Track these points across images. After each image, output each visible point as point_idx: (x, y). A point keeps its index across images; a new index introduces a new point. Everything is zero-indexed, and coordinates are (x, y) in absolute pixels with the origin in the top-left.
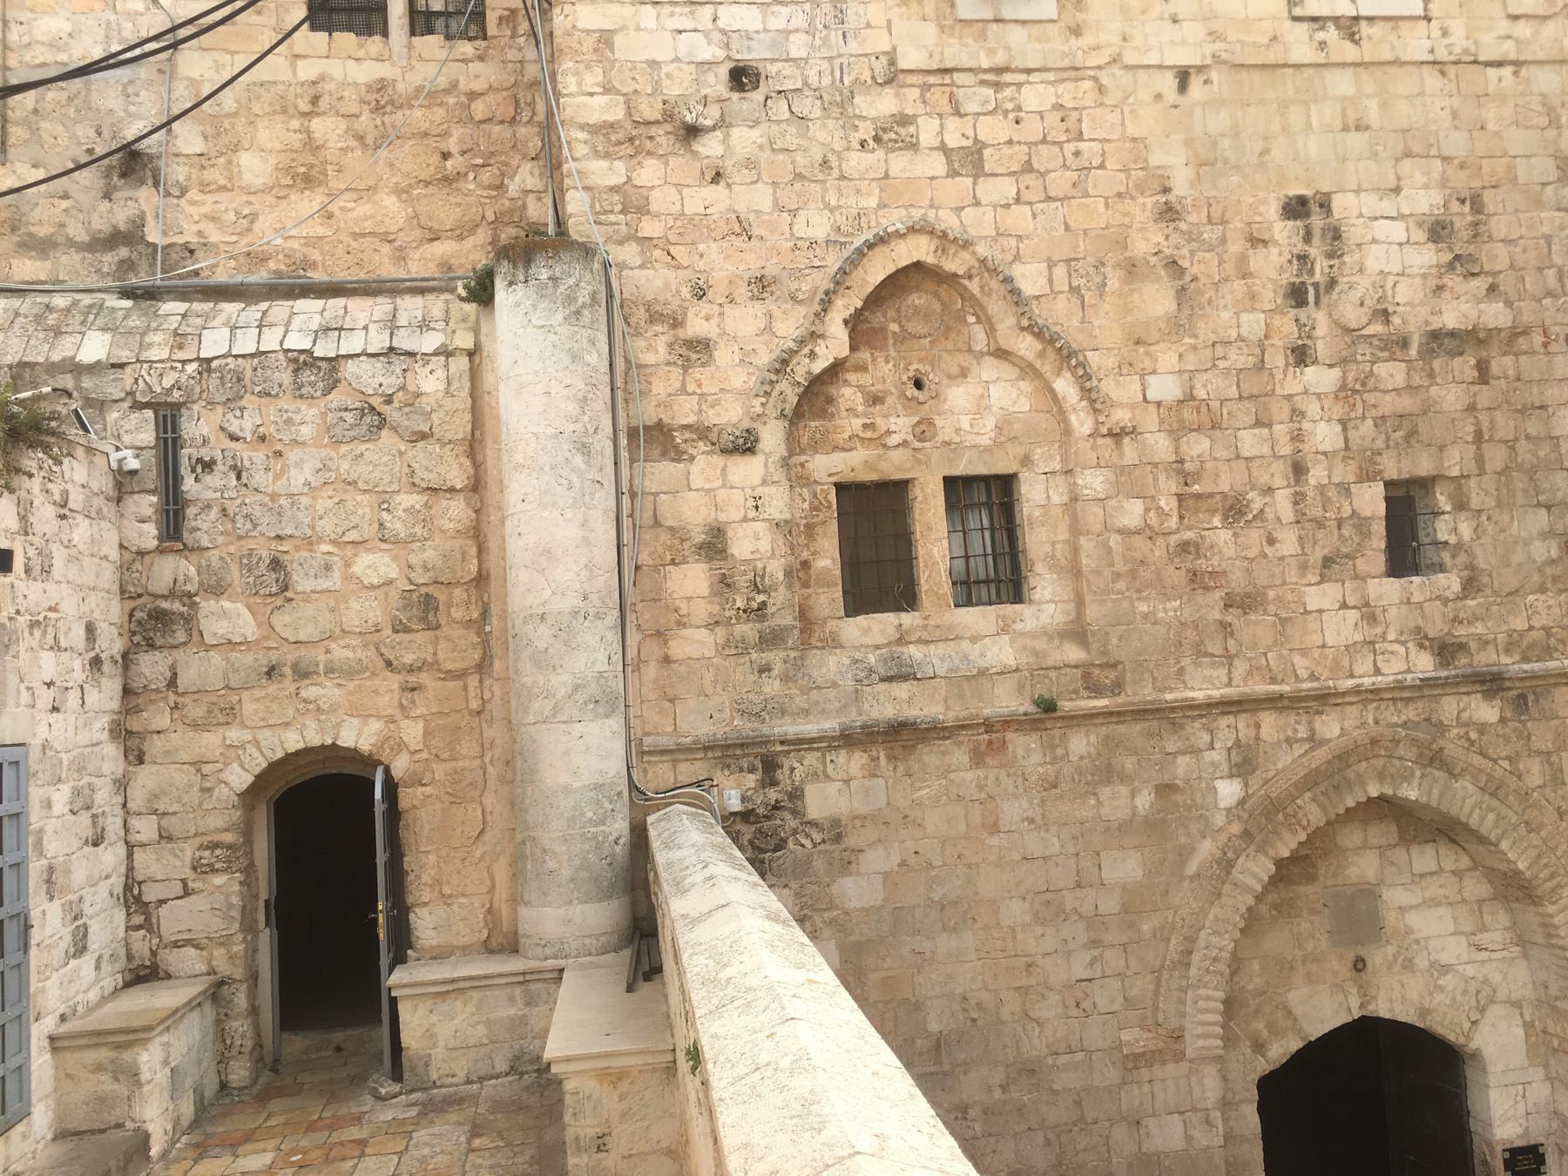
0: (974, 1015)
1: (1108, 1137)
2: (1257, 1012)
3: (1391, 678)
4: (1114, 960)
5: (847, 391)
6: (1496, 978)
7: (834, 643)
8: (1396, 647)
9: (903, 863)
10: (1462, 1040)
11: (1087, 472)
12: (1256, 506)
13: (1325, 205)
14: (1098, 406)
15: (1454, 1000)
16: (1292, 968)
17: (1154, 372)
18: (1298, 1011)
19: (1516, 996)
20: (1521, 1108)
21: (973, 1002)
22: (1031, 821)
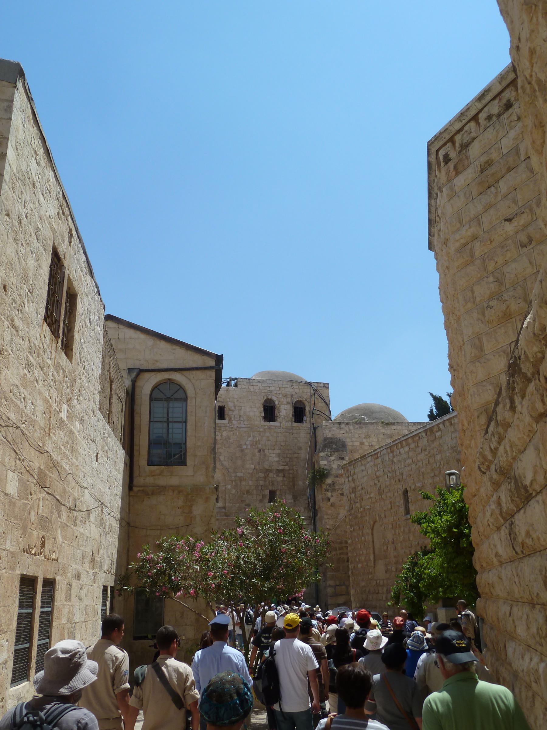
13: (264, 451)
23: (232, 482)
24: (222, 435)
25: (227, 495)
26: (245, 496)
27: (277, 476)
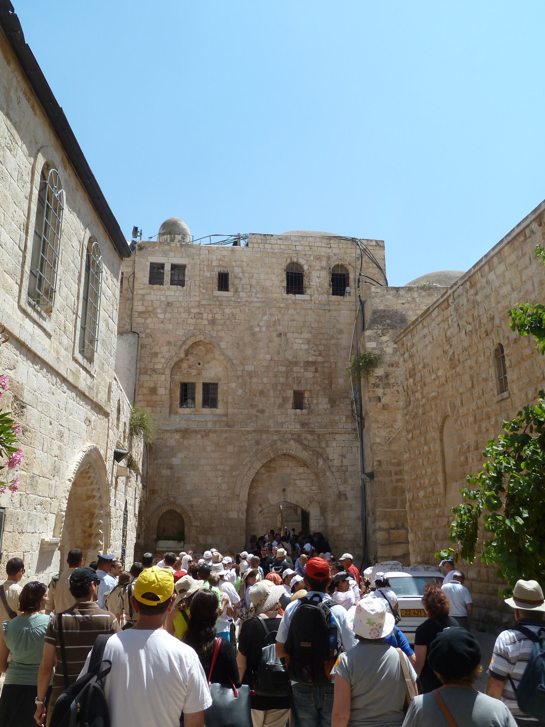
0: (196, 487)
4: (226, 480)
5: (184, 364)
7: (176, 413)
8: (293, 423)
9: (185, 456)
13: (286, 335)
16: (269, 490)
20: (318, 524)
22: (212, 451)
23: (238, 378)
24: (224, 313)
25: (229, 397)
26: (257, 398)
27: (306, 370)
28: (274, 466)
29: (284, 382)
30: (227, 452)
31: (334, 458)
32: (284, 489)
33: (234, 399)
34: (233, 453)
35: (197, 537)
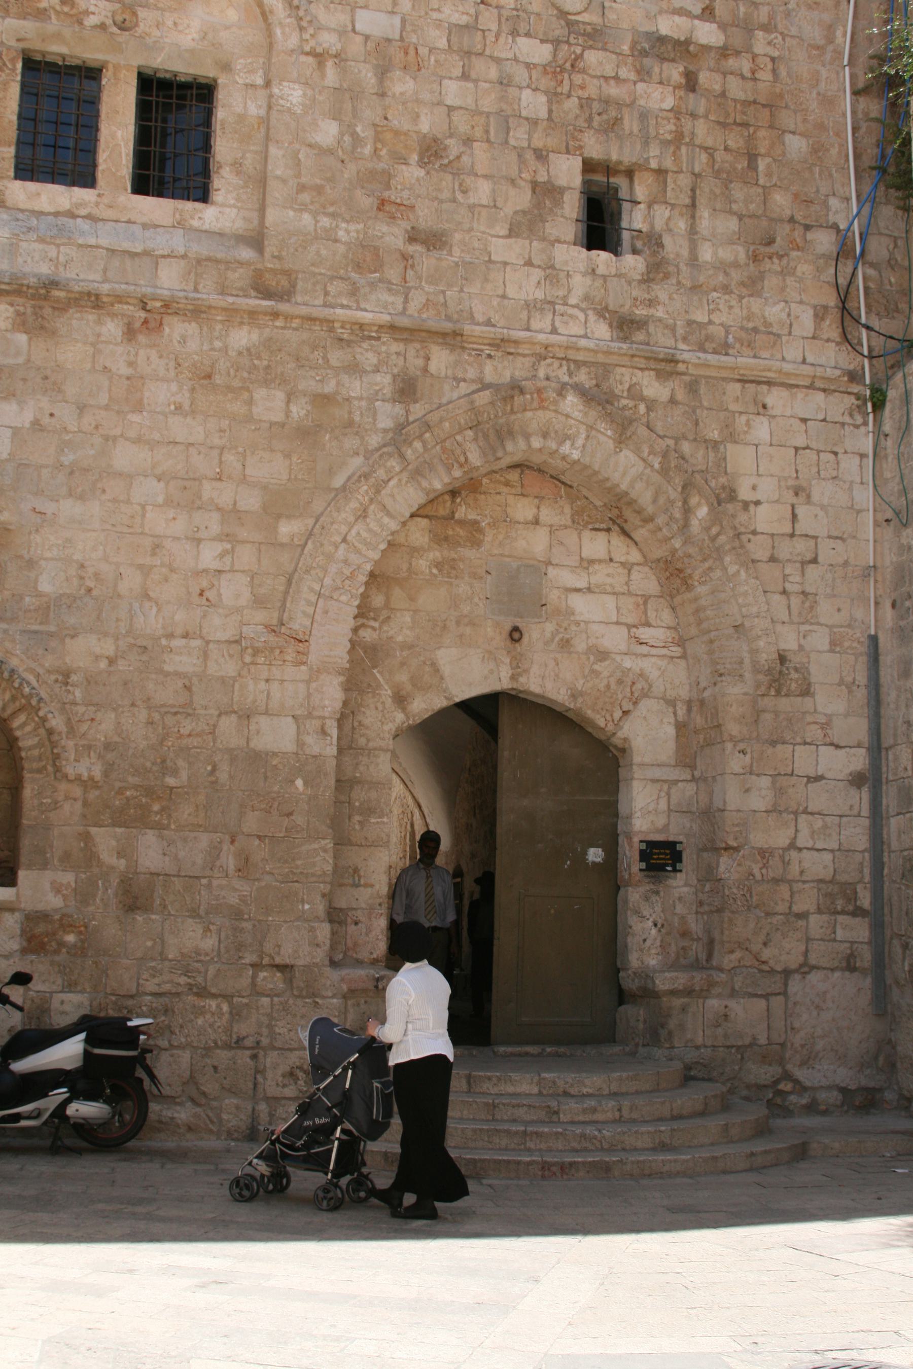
0: (91, 584)
1: (215, 726)
2: (403, 664)
3: (564, 338)
4: (246, 556)
6: (654, 674)
8: (576, 312)
9: (36, 424)
10: (610, 728)
11: (285, 84)
12: (453, 152)
14: (304, 24)
15: (608, 687)
16: (445, 627)
17: (366, 7)
18: (446, 670)
19: (671, 694)
20: (663, 805)
21: (91, 570)
22: (179, 407)
23: (321, 65)
27: (643, 74)
28: (472, 516)
29: (543, 114)
30: (249, 418)
31: (758, 496)
32: (516, 629)
33: (298, 163)
34: (283, 425)
35: (87, 838)
